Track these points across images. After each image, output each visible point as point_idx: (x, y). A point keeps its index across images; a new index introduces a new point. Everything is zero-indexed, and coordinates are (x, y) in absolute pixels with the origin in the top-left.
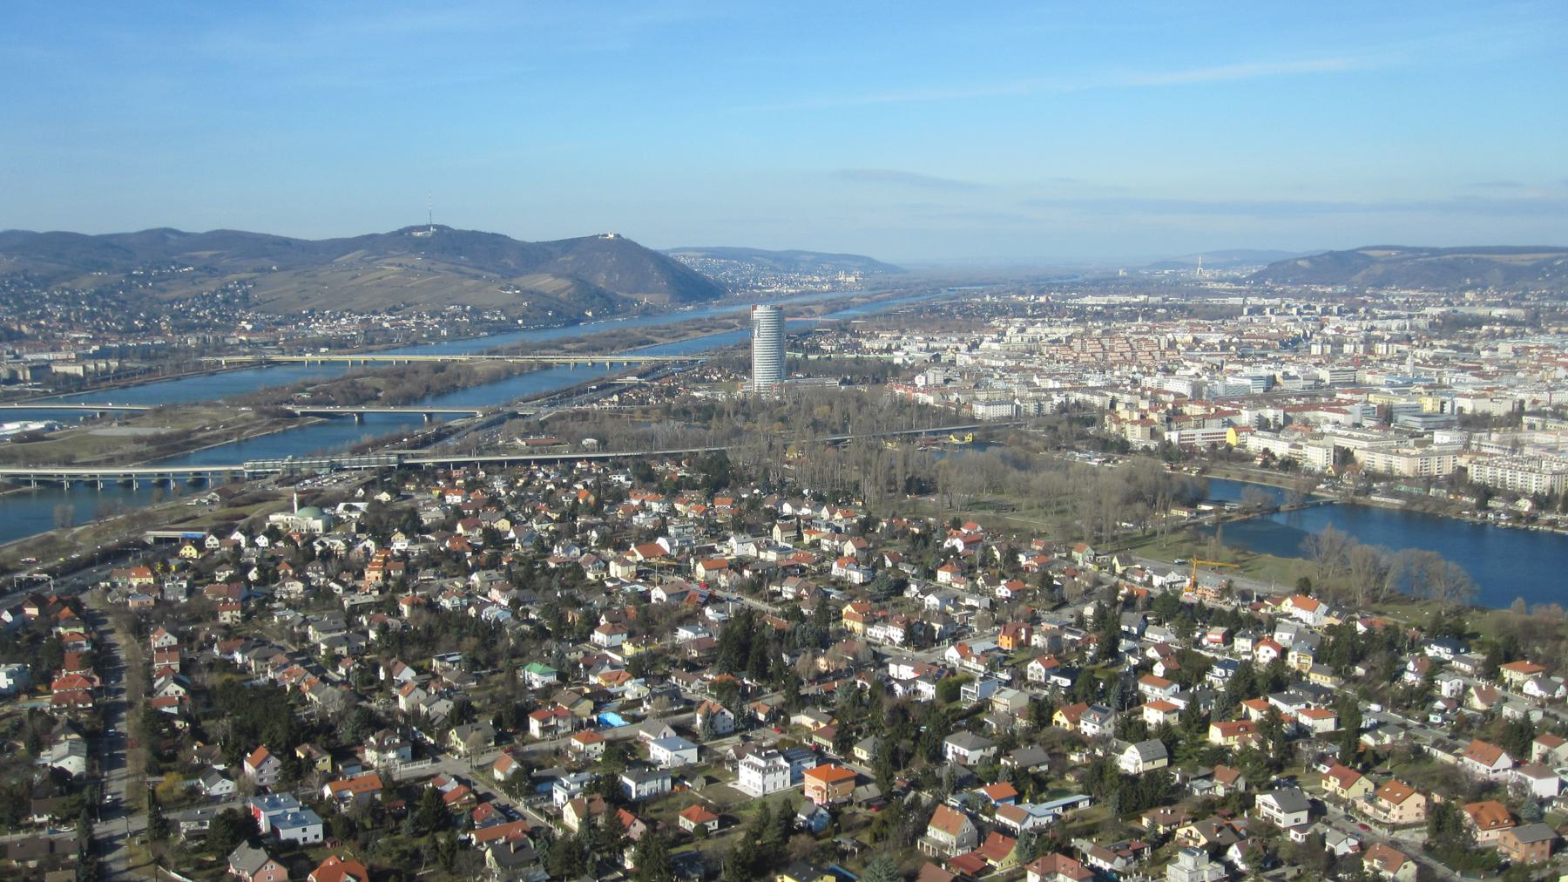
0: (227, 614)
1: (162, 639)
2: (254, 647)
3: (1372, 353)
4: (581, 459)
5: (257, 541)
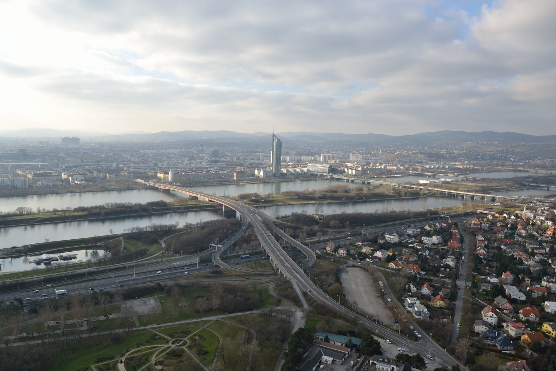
0: (500, 235)
1: (480, 238)
2: (508, 245)
5: (511, 217)
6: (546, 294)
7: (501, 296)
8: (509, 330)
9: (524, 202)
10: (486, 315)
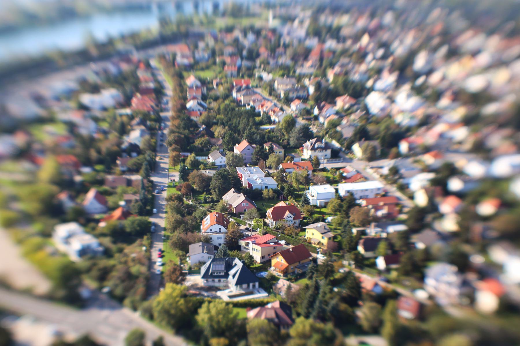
2: (243, 90)
7: (233, 190)
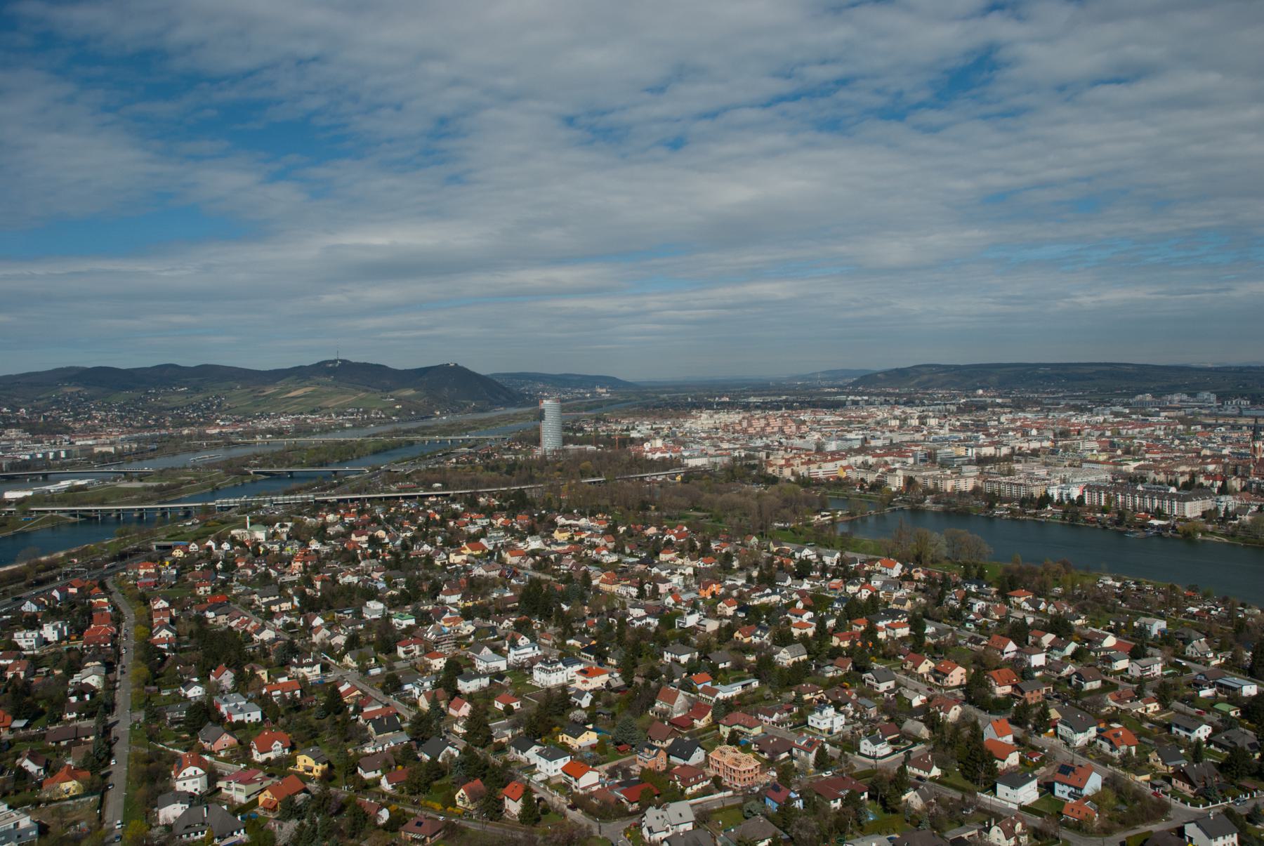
0: (202, 589)
3: (924, 424)
4: (431, 496)
6: (298, 692)
8: (233, 793)
9: (246, 509)
10: (181, 776)
